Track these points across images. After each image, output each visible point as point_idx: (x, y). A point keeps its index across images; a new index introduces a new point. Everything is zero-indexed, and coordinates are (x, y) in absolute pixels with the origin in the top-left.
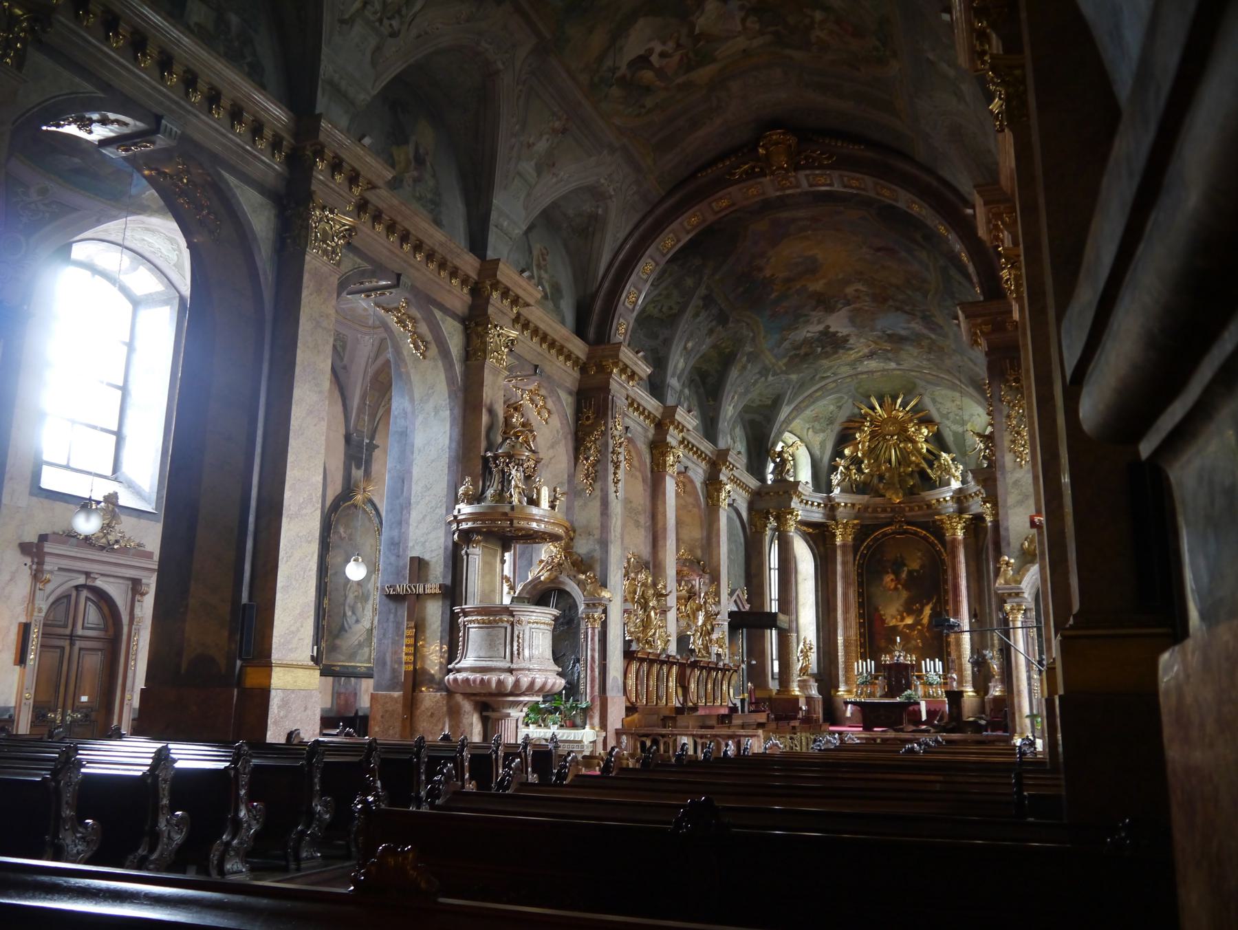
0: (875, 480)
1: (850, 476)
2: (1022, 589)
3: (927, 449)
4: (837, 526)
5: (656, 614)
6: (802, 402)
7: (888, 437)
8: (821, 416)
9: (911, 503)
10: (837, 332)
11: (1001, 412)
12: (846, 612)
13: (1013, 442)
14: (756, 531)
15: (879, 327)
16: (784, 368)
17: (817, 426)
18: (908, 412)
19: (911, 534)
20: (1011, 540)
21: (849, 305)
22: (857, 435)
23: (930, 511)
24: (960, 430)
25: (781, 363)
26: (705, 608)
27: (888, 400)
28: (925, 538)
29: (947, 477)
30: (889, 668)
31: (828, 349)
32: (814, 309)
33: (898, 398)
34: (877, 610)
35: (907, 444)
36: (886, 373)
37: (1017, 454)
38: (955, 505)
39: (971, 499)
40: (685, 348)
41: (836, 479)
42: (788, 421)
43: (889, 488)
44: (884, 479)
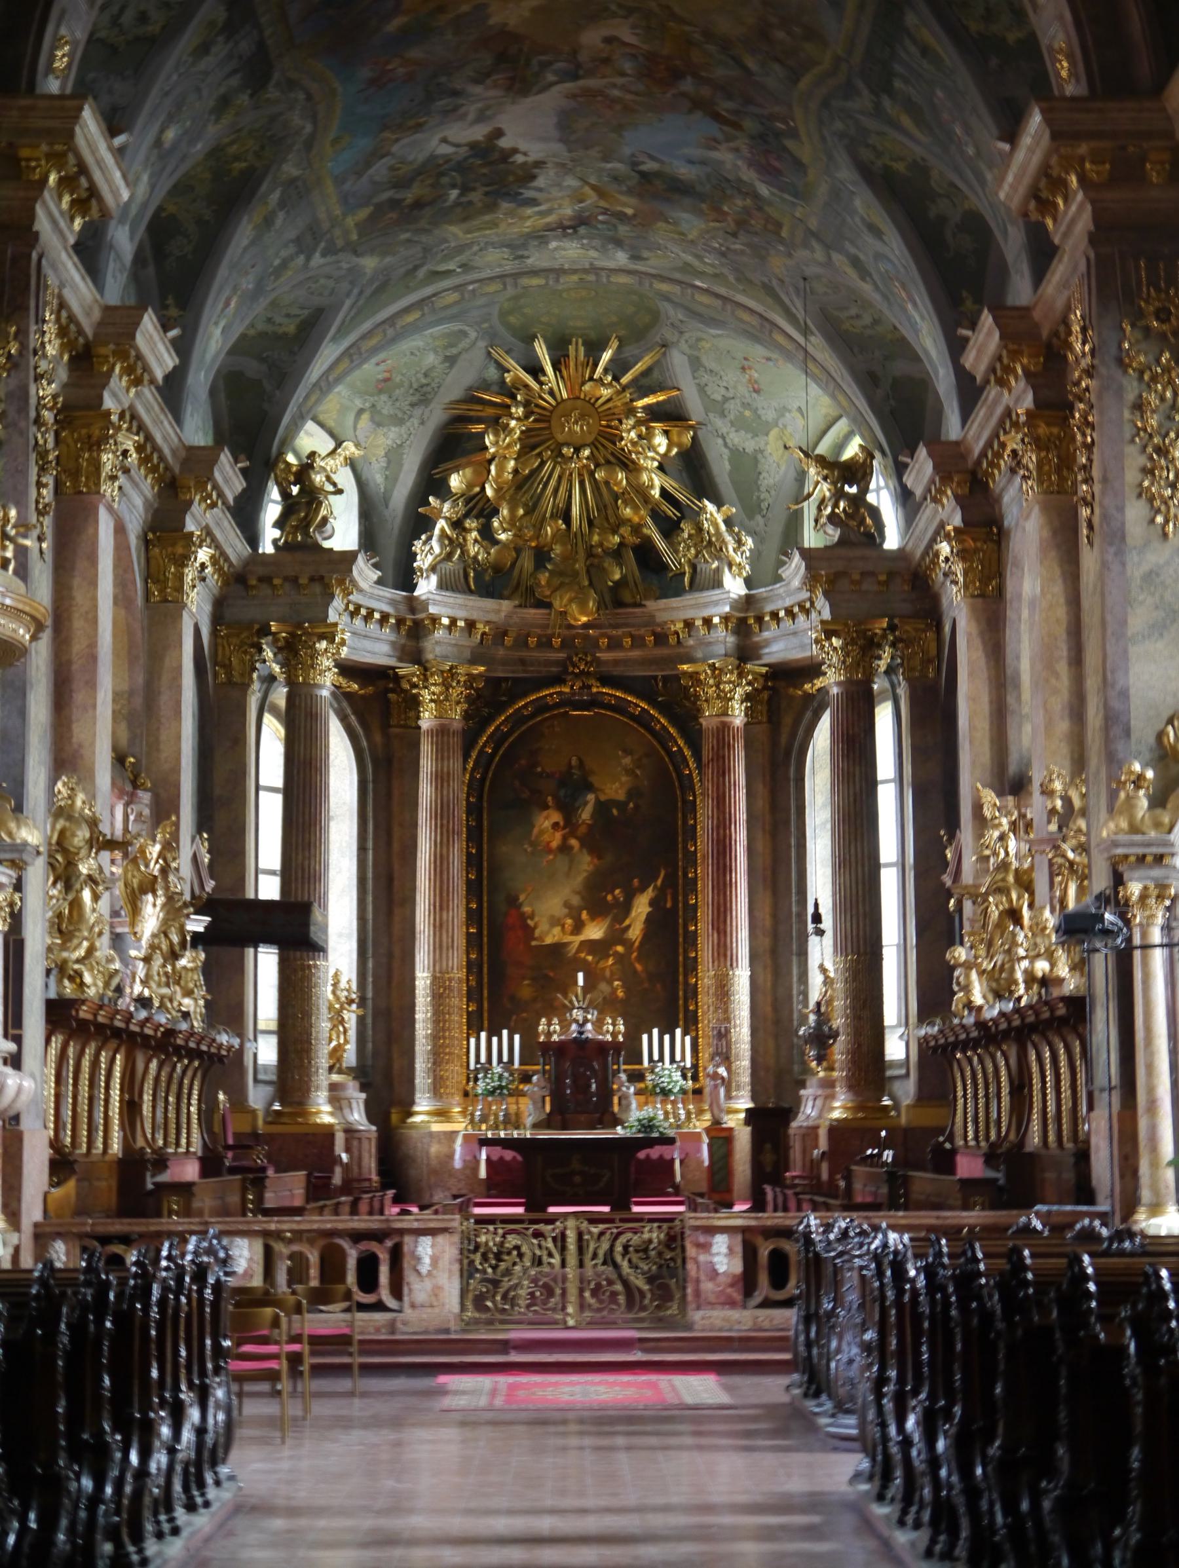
0: (527, 562)
1: (463, 547)
2: (1172, 845)
3: (664, 492)
4: (426, 679)
5: (96, 897)
6: (364, 337)
7: (568, 451)
8: (398, 379)
9: (616, 626)
10: (515, 151)
11: (1120, 392)
12: (441, 904)
13: (1148, 472)
14: (230, 682)
15: (627, 151)
16: (354, 237)
17: (386, 407)
18: (624, 388)
19: (609, 707)
20: (1133, 722)
21: (575, 77)
22: (489, 440)
23: (663, 652)
24: (750, 445)
25: (350, 221)
26: (167, 888)
27: (577, 351)
28: (643, 720)
29: (715, 565)
30: (560, 1050)
31: (476, 197)
32: (480, 79)
33: (604, 350)
34: (513, 902)
35: (613, 473)
36: (591, 278)
37: (1157, 503)
38: (731, 639)
39: (774, 625)
40: (158, 143)
41: (427, 552)
42: (325, 386)
43: (562, 585)
44: (550, 559)
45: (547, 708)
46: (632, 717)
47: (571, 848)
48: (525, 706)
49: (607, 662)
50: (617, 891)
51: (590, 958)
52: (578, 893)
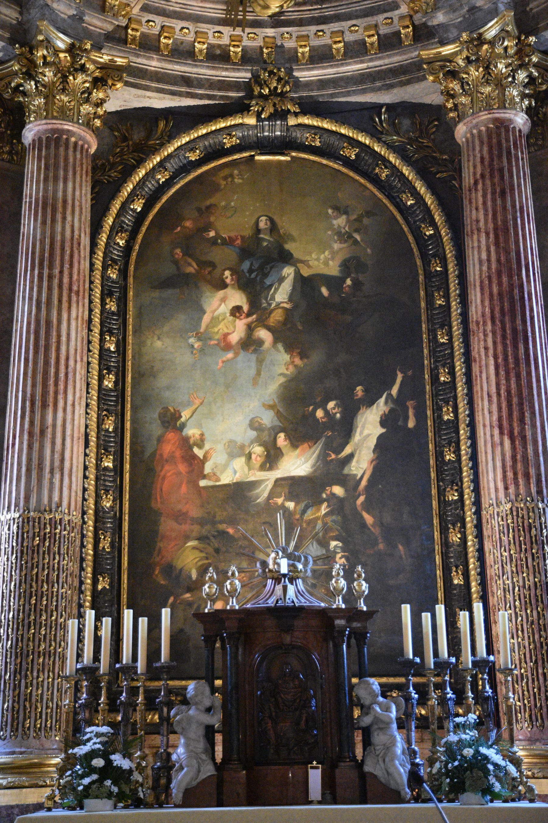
45: (221, 152)
46: (346, 162)
47: (260, 342)
48: (190, 146)
49: (308, 85)
50: (331, 405)
51: (291, 505)
52: (271, 407)
